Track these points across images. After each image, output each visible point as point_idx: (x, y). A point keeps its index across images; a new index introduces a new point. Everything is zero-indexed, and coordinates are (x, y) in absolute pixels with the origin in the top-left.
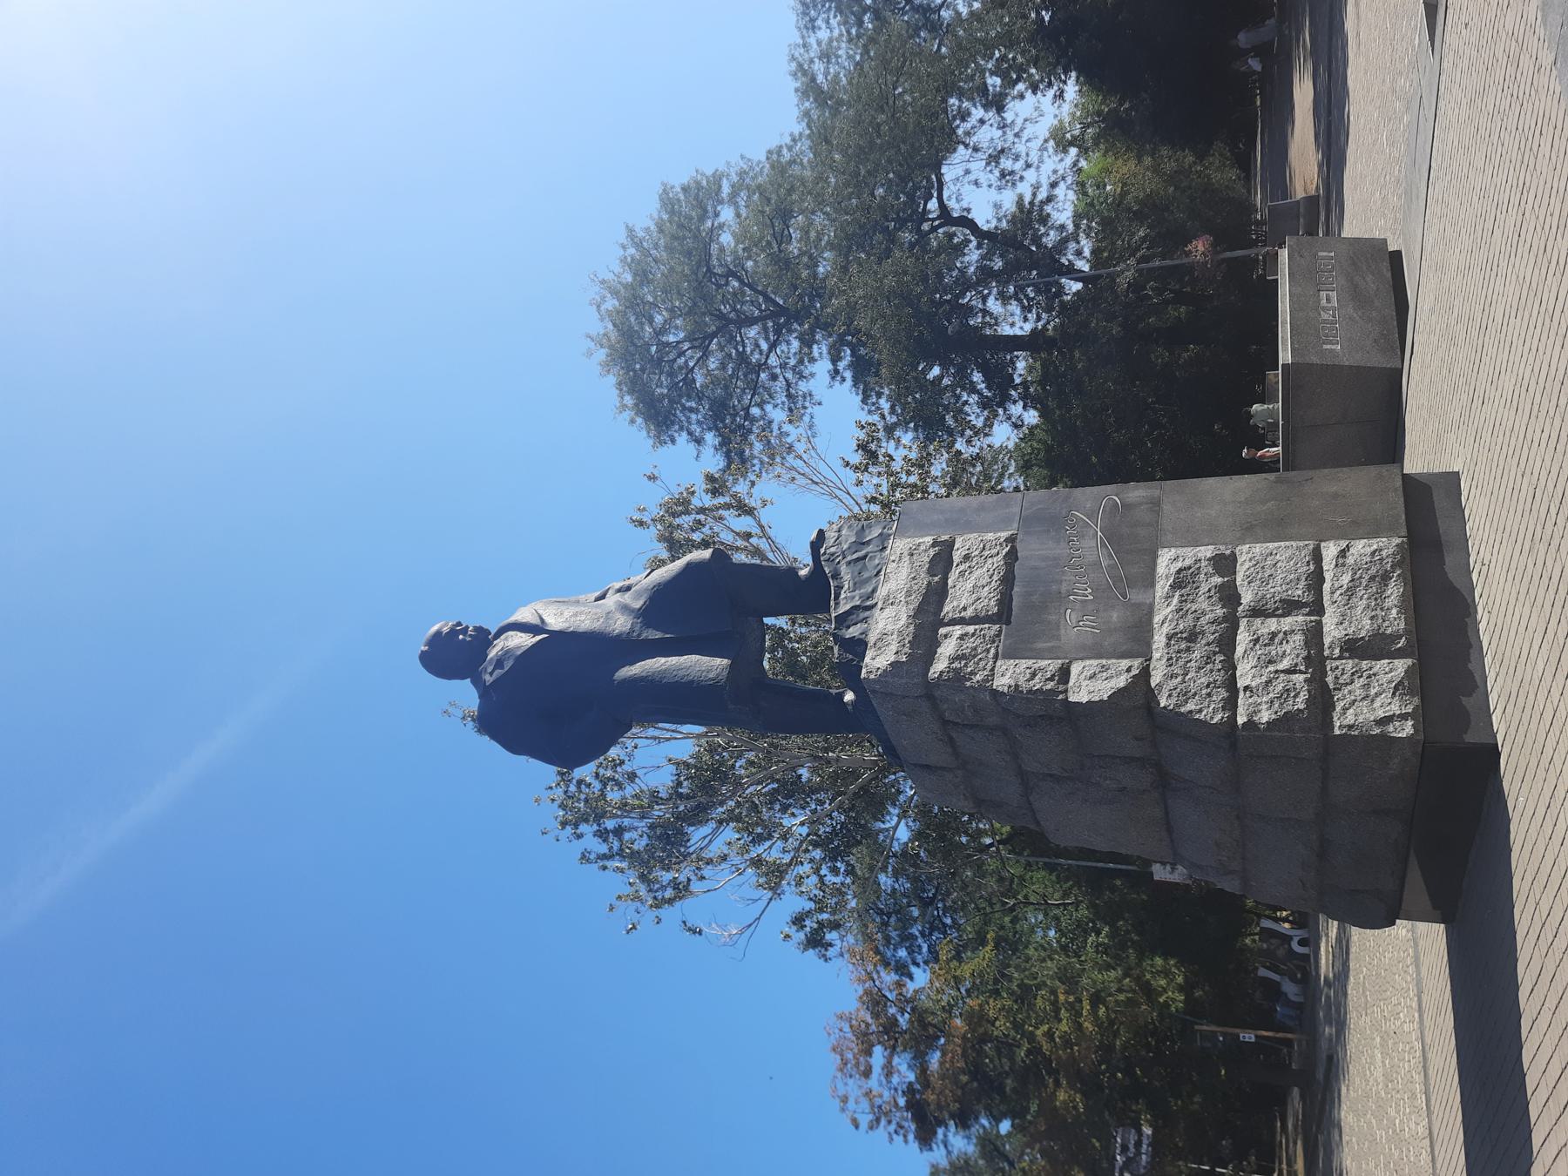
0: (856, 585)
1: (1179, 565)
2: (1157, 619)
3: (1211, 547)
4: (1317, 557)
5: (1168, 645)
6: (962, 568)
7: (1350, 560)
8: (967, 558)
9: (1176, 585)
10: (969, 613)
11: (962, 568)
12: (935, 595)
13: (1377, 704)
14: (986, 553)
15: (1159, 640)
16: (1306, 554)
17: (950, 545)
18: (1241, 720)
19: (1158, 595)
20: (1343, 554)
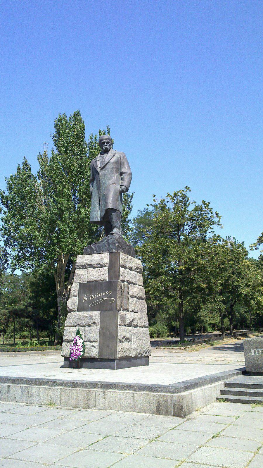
0: (99, 247)
1: (94, 315)
2: (84, 312)
3: (99, 321)
4: (95, 342)
5: (78, 315)
6: (99, 271)
7: (92, 348)
8: (101, 271)
9: (90, 316)
10: (88, 275)
11: (99, 271)
12: (92, 266)
13: (67, 350)
14: (102, 275)
15: (81, 313)
16: (95, 340)
17: (106, 267)
18: (65, 328)
19: (88, 312)
20: (94, 346)
